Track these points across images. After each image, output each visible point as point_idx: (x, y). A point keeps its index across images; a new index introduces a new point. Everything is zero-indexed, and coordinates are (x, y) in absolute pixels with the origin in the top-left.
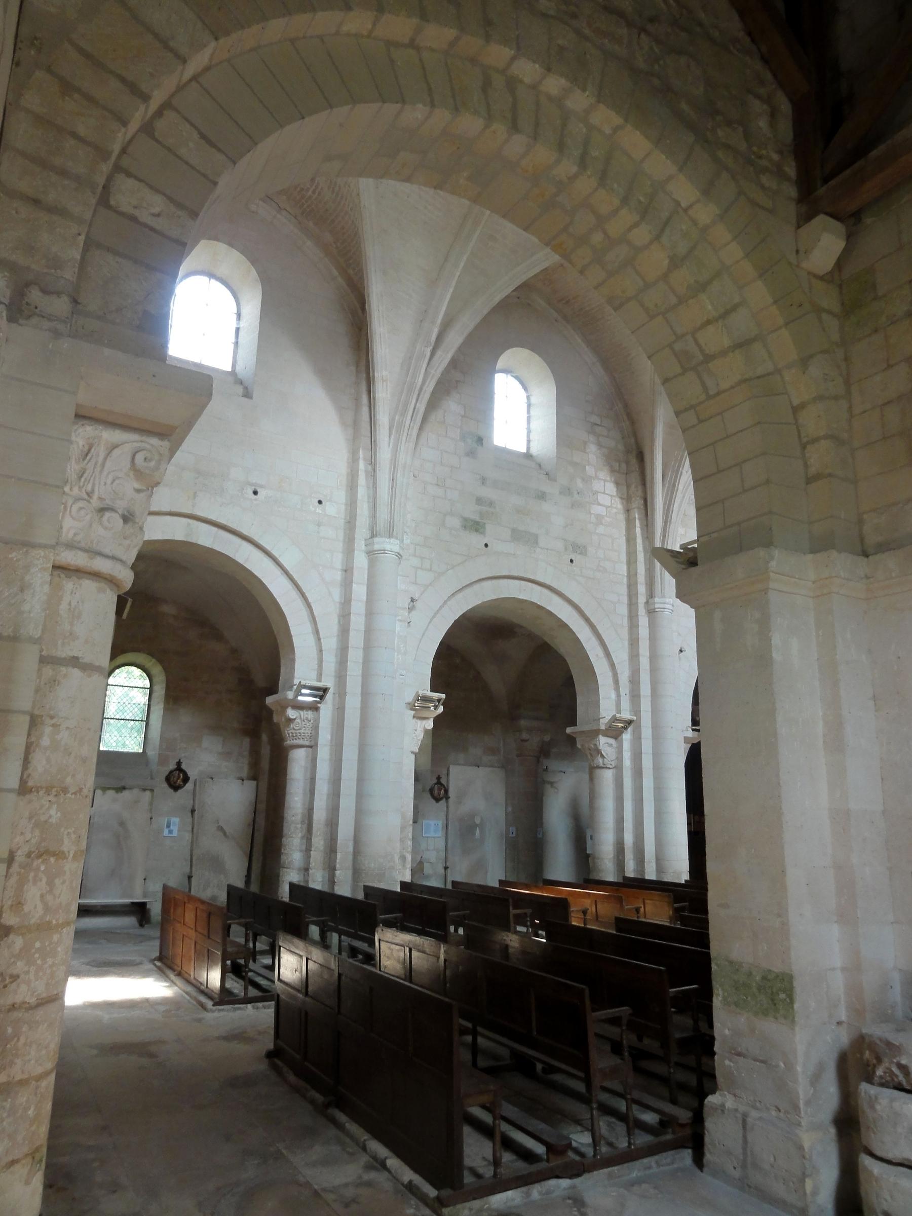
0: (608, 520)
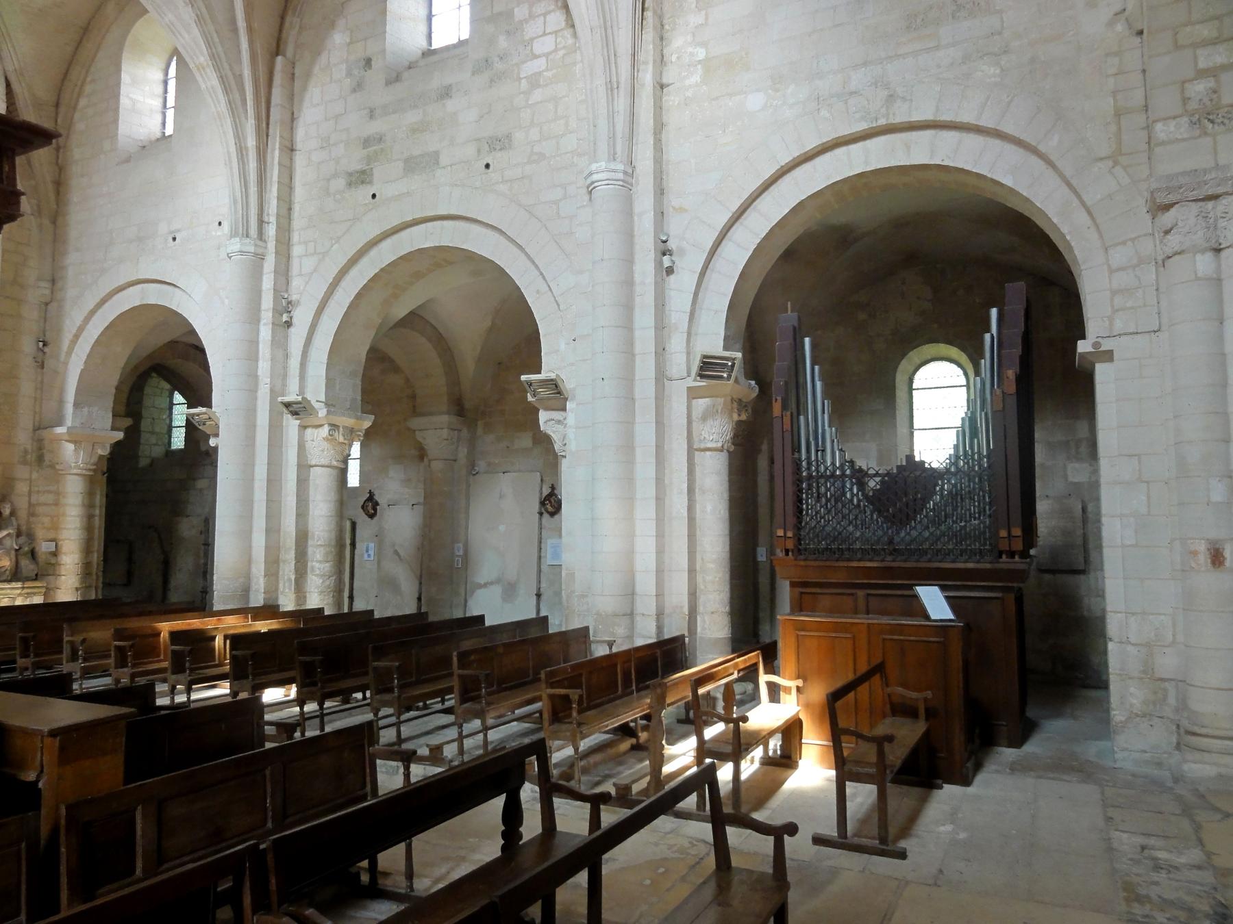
0: (549, 74)
